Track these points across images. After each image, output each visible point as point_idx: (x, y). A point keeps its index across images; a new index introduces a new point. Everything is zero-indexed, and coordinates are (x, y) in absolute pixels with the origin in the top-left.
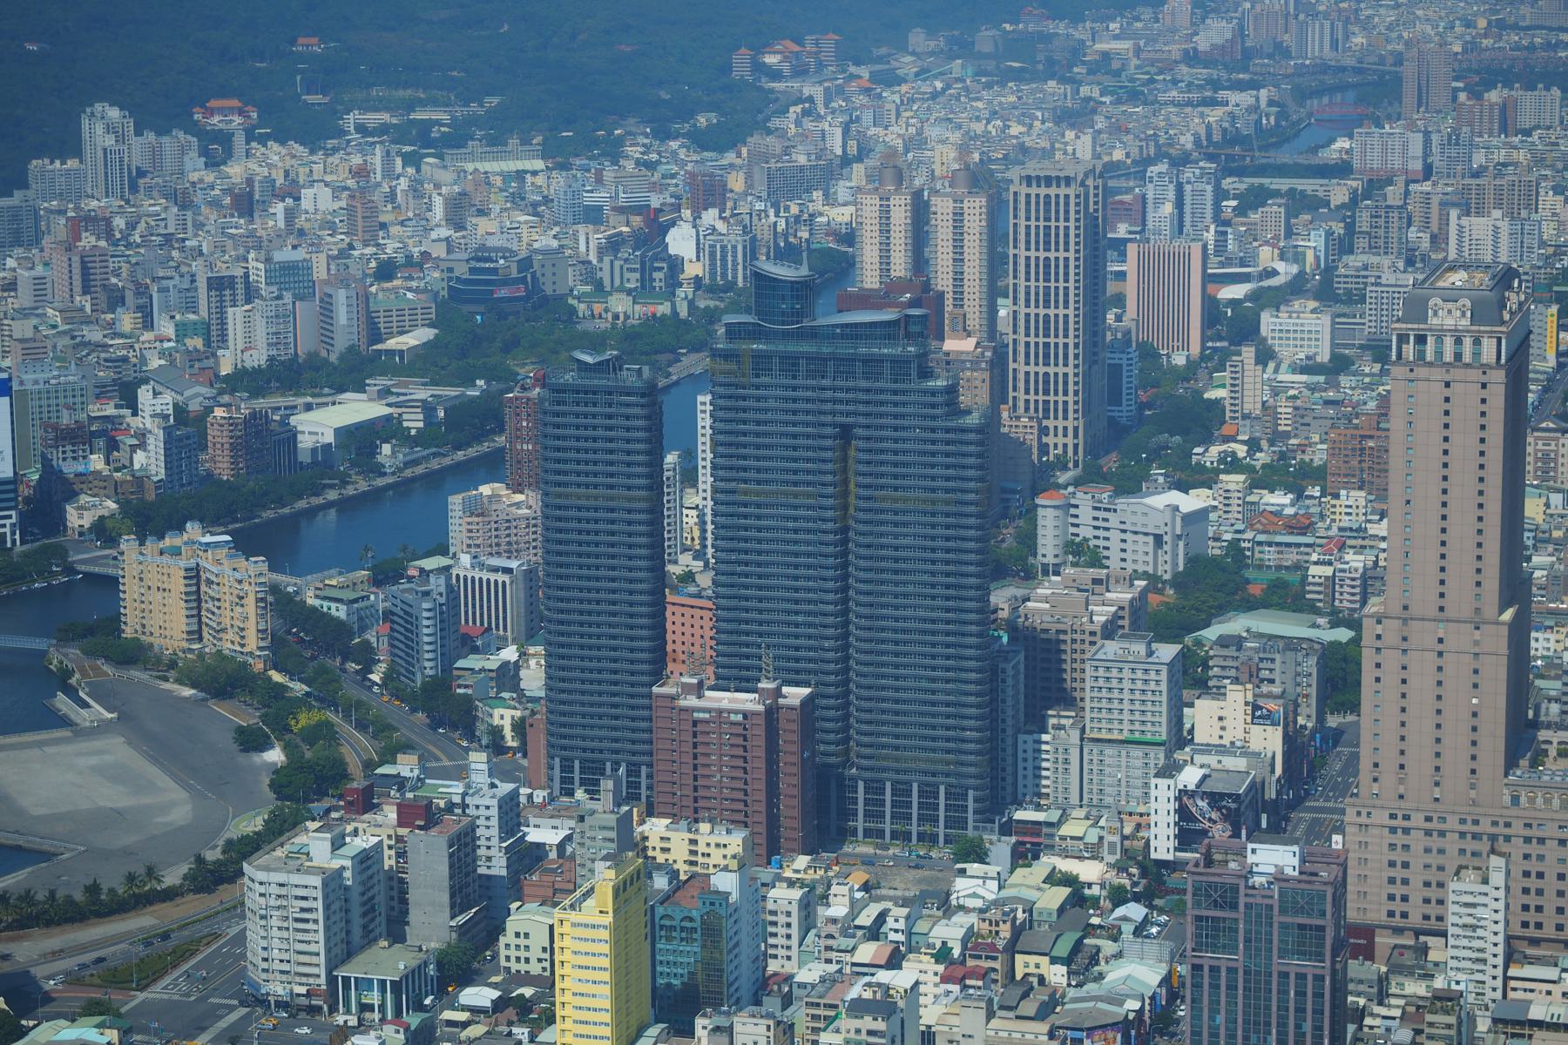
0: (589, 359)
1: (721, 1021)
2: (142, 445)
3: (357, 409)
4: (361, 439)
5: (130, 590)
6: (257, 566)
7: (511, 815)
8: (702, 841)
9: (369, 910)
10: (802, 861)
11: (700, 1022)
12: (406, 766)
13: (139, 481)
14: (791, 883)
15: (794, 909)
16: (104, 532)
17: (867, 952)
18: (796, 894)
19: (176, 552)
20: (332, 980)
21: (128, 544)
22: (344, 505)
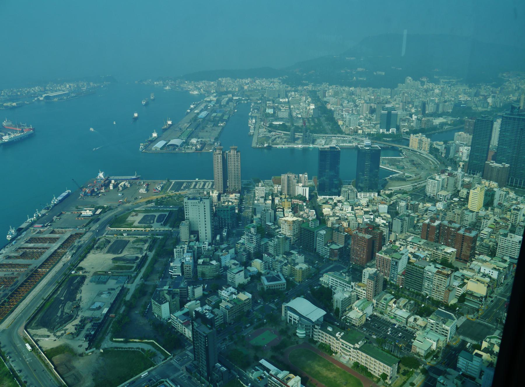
0: (484, 116)
1: (493, 208)
2: (413, 122)
3: (441, 120)
4: (442, 124)
5: (411, 141)
6: (429, 140)
7: (463, 176)
8: (491, 183)
9: (443, 186)
10: (504, 188)
11: (489, 208)
12: (449, 168)
13: (412, 127)
14: (504, 191)
15: (504, 195)
16: (408, 133)
17: (514, 202)
18: (505, 193)
19: (418, 137)
20: (437, 194)
21: (412, 135)
22: (439, 133)
